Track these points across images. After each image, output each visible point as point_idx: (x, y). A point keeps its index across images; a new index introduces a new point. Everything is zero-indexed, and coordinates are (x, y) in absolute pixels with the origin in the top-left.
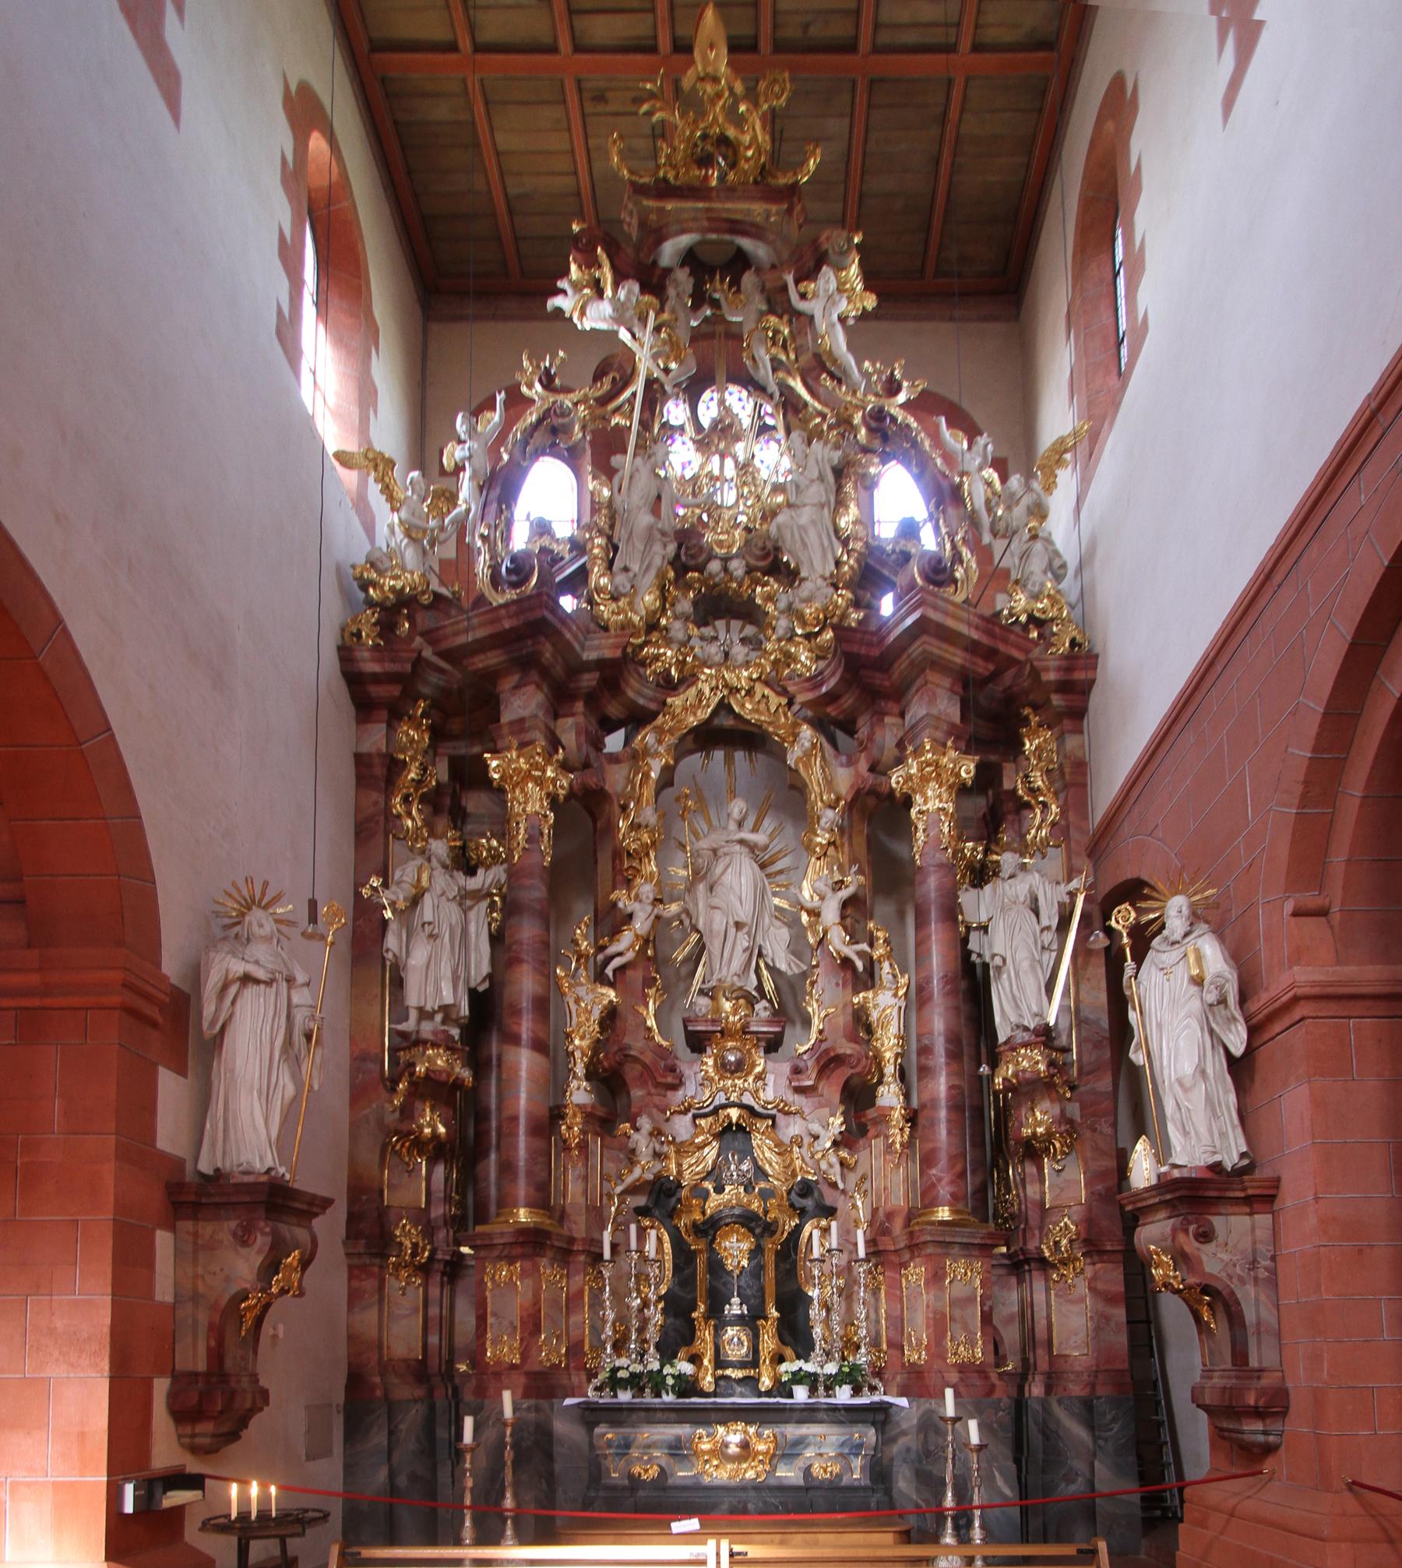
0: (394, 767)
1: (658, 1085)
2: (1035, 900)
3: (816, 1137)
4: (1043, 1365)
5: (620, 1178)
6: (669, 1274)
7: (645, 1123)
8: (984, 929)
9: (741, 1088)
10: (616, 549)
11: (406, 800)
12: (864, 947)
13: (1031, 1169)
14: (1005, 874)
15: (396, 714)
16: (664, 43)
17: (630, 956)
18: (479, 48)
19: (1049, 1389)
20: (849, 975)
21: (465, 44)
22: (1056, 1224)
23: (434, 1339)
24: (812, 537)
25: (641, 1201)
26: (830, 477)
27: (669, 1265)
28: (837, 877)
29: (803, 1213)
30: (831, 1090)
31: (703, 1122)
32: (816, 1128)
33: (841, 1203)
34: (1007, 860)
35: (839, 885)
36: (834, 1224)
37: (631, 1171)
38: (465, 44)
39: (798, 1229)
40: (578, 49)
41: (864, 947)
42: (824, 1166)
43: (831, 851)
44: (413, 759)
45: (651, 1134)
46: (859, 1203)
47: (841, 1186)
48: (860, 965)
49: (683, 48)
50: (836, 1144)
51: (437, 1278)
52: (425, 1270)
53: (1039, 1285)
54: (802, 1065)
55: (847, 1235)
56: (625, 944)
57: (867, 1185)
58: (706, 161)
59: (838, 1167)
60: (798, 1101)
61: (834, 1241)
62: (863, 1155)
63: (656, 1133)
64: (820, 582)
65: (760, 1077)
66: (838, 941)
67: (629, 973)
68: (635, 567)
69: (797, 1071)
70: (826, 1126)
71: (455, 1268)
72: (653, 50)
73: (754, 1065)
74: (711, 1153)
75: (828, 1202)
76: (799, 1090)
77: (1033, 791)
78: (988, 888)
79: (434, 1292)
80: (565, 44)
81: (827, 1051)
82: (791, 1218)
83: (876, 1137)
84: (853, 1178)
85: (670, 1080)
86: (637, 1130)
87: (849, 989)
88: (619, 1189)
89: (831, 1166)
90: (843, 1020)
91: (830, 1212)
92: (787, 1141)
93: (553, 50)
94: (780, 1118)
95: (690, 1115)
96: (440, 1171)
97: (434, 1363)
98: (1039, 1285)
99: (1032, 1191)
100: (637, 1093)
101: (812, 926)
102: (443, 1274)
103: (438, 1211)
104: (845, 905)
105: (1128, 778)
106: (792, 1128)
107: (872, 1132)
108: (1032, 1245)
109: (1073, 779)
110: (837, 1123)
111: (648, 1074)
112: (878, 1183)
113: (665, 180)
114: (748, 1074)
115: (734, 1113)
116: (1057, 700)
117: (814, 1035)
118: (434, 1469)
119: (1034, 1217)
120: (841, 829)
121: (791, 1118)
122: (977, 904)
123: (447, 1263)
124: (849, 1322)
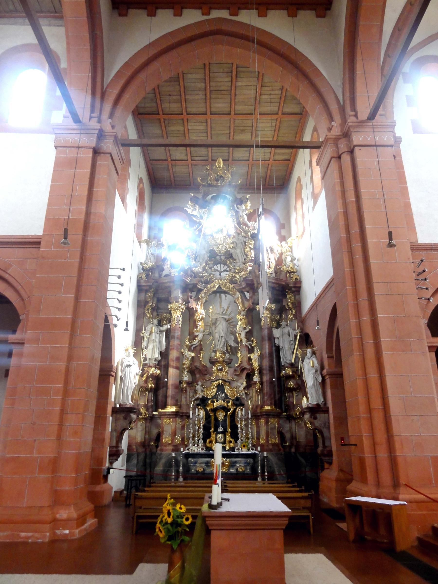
0: (147, 303)
1: (203, 374)
2: (289, 332)
3: (240, 387)
4: (295, 443)
5: (194, 397)
6: (204, 420)
7: (200, 383)
8: (278, 338)
9: (220, 375)
10: (197, 257)
11: (148, 310)
12: (251, 343)
13: (291, 394)
14: (283, 326)
15: (147, 291)
16: (210, 160)
17: (197, 345)
18: (172, 160)
19: (296, 450)
20: (247, 349)
21: (169, 160)
22: (296, 408)
23: (147, 436)
24: (239, 255)
25: (198, 402)
26: (243, 243)
27: (205, 418)
28: (245, 326)
29: (237, 406)
30: (244, 376)
31: (214, 383)
32: (239, 384)
33: (246, 403)
34: (283, 323)
35: (245, 329)
36: (244, 409)
37: (196, 395)
38: (169, 160)
39: (235, 410)
40: (192, 160)
41: (251, 343)
42: (241, 394)
43: (244, 321)
44: (150, 300)
45: (201, 386)
46: (250, 404)
47: (245, 399)
48: (250, 347)
49: (214, 161)
50: (244, 388)
51: (148, 421)
52: (145, 419)
53: (293, 423)
54: (236, 369)
55: (247, 413)
56: (196, 342)
57: (251, 399)
58: (217, 180)
59: (245, 395)
60: (235, 378)
61: (243, 413)
62: (251, 391)
63: (202, 386)
64: (241, 263)
65: (226, 372)
66: (244, 341)
67: (197, 348)
68: (201, 261)
69: (235, 371)
70: (242, 384)
71: (152, 418)
72: (208, 160)
73: (225, 369)
74: (215, 391)
75: (243, 402)
76: (235, 375)
77: (289, 307)
78: (279, 329)
79: (148, 424)
80: (190, 160)
81: (242, 367)
82: (234, 406)
83: (254, 387)
84: (249, 397)
85: (206, 373)
86: (198, 385)
87: (247, 353)
88: (193, 399)
89: (243, 394)
90: (246, 359)
91: (243, 405)
92: (232, 387)
93: (187, 160)
94: (231, 382)
95: (210, 381)
96: (150, 394)
97: (147, 442)
98: (293, 423)
99: (291, 399)
100: (198, 376)
101: (239, 336)
102: (150, 420)
103: (150, 404)
104: (247, 333)
105: (308, 310)
106: (235, 384)
107: (253, 387)
108: (291, 413)
109: (298, 305)
110: (245, 383)
111: (200, 372)
112: (253, 399)
113: (209, 184)
114: (224, 371)
115: (221, 381)
116: (293, 289)
117: (239, 362)
118: (145, 470)
119: (292, 407)
120: (246, 316)
121: (234, 382)
122: (276, 333)
123: (151, 417)
124: (247, 434)
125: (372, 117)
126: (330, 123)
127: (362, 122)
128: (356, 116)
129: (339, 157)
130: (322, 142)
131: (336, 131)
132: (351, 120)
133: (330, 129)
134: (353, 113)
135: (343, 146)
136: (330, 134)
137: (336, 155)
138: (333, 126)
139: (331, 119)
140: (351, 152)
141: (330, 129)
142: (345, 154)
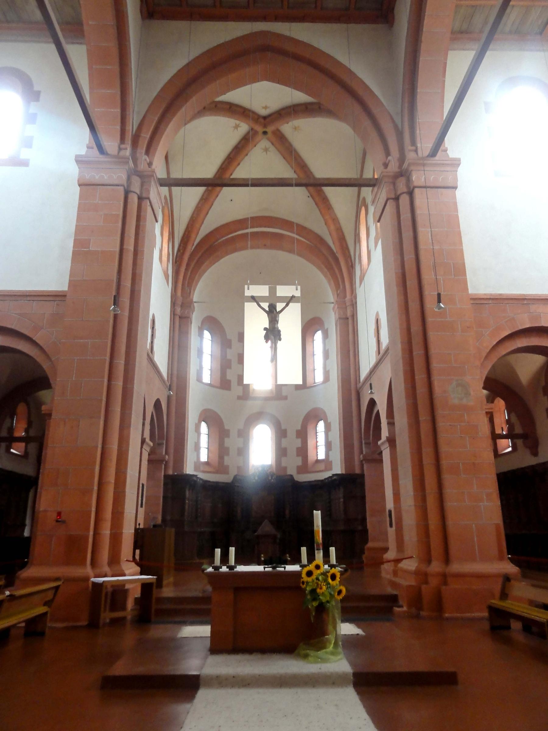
125: (434, 153)
126: (387, 158)
127: (423, 158)
128: (416, 151)
129: (397, 199)
130: (377, 179)
131: (393, 167)
132: (410, 156)
133: (386, 165)
134: (413, 148)
135: (401, 186)
136: (385, 170)
137: (393, 196)
138: (389, 161)
139: (388, 153)
140: (411, 194)
141: (386, 165)
142: (405, 195)
